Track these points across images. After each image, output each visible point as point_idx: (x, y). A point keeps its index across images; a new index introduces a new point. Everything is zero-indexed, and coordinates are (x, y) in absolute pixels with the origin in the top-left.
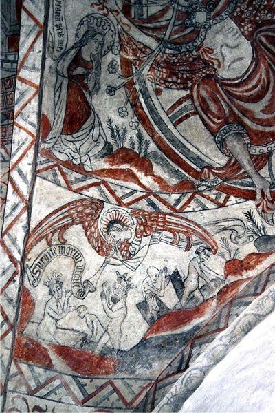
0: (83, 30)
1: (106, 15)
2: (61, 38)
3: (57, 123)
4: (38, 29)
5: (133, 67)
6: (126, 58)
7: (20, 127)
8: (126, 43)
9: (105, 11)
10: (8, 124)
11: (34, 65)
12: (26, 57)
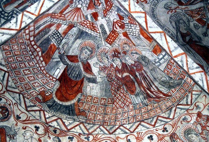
0: (174, 24)
1: (176, 12)
2: (170, 33)
3: (202, 62)
4: (163, 34)
5: (203, 19)
6: (197, 19)
7: (194, 73)
8: (192, 14)
9: (174, 11)
10: (185, 81)
11: (175, 47)
12: (169, 48)
